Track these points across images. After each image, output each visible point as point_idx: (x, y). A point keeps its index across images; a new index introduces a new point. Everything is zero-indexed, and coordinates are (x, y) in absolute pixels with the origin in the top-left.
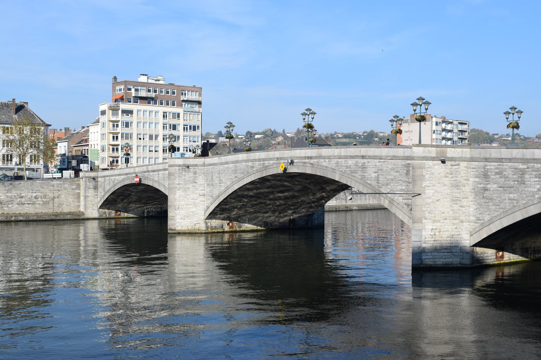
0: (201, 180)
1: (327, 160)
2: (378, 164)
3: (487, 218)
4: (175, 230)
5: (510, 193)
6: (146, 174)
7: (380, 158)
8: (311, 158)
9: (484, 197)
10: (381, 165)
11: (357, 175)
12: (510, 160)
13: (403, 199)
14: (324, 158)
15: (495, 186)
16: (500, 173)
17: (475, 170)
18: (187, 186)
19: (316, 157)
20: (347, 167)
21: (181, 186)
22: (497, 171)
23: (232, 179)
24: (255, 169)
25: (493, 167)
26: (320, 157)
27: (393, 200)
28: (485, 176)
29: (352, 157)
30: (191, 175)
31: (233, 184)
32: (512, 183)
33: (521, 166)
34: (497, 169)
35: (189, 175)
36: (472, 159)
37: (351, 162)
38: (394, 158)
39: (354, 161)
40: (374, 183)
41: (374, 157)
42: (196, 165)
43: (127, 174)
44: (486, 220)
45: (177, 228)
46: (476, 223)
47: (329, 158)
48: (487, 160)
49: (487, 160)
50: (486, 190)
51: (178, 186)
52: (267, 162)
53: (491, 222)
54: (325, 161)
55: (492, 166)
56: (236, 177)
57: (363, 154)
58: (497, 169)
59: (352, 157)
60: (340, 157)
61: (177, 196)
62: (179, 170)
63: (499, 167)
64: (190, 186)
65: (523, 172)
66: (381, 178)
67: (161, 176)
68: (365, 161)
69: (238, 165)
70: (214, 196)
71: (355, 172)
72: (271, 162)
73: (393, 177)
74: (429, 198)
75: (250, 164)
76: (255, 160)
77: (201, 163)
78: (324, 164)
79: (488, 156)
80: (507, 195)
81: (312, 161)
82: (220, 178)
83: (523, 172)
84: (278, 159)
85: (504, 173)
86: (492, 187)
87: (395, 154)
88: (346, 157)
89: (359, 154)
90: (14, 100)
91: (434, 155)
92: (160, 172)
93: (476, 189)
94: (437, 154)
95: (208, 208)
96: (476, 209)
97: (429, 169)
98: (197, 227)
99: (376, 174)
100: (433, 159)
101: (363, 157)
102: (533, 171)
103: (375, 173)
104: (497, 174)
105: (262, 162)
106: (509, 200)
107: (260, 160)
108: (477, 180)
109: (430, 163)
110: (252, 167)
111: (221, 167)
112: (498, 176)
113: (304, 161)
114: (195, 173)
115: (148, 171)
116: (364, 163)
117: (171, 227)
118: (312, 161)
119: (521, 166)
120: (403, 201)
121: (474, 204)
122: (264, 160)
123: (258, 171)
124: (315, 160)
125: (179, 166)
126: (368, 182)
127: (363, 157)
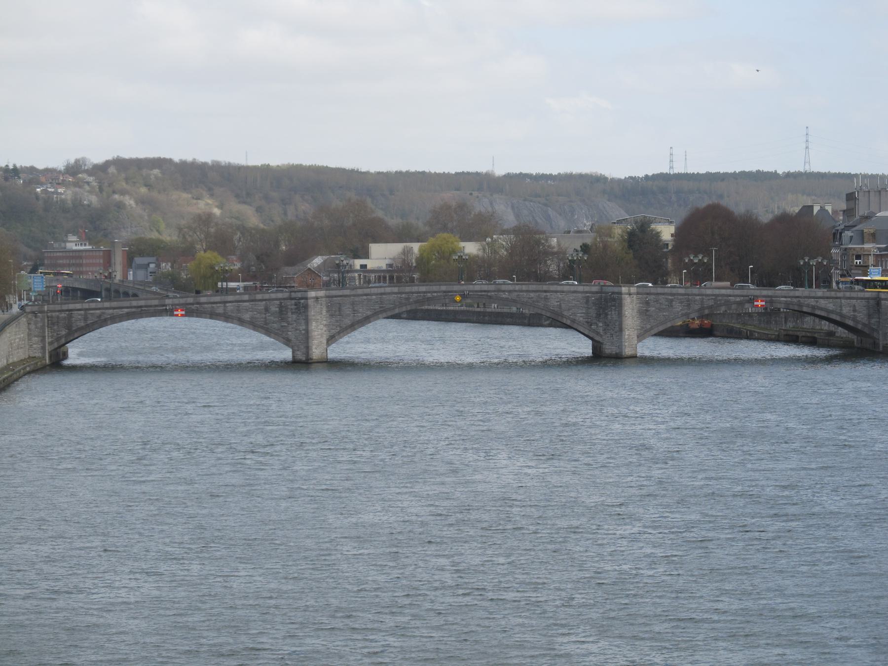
2: (560, 296)
3: (649, 326)
6: (194, 307)
7: (563, 292)
8: (488, 291)
9: (646, 315)
12: (663, 294)
14: (504, 291)
16: (657, 301)
19: (494, 291)
20: (529, 298)
24: (411, 300)
28: (647, 303)
32: (664, 307)
33: (670, 297)
37: (532, 295)
40: (556, 309)
41: (556, 292)
43: (141, 307)
47: (510, 292)
48: (648, 294)
49: (648, 294)
50: (647, 311)
55: (652, 297)
65: (672, 301)
66: (563, 306)
68: (548, 294)
69: (384, 296)
70: (344, 326)
72: (435, 294)
76: (413, 293)
78: (504, 296)
81: (489, 294)
83: (672, 301)
84: (445, 292)
92: (228, 305)
101: (545, 291)
104: (654, 302)
110: (408, 299)
111: (357, 299)
113: (480, 293)
115: (198, 303)
118: (489, 294)
119: (670, 297)
122: (425, 292)
127: (545, 291)
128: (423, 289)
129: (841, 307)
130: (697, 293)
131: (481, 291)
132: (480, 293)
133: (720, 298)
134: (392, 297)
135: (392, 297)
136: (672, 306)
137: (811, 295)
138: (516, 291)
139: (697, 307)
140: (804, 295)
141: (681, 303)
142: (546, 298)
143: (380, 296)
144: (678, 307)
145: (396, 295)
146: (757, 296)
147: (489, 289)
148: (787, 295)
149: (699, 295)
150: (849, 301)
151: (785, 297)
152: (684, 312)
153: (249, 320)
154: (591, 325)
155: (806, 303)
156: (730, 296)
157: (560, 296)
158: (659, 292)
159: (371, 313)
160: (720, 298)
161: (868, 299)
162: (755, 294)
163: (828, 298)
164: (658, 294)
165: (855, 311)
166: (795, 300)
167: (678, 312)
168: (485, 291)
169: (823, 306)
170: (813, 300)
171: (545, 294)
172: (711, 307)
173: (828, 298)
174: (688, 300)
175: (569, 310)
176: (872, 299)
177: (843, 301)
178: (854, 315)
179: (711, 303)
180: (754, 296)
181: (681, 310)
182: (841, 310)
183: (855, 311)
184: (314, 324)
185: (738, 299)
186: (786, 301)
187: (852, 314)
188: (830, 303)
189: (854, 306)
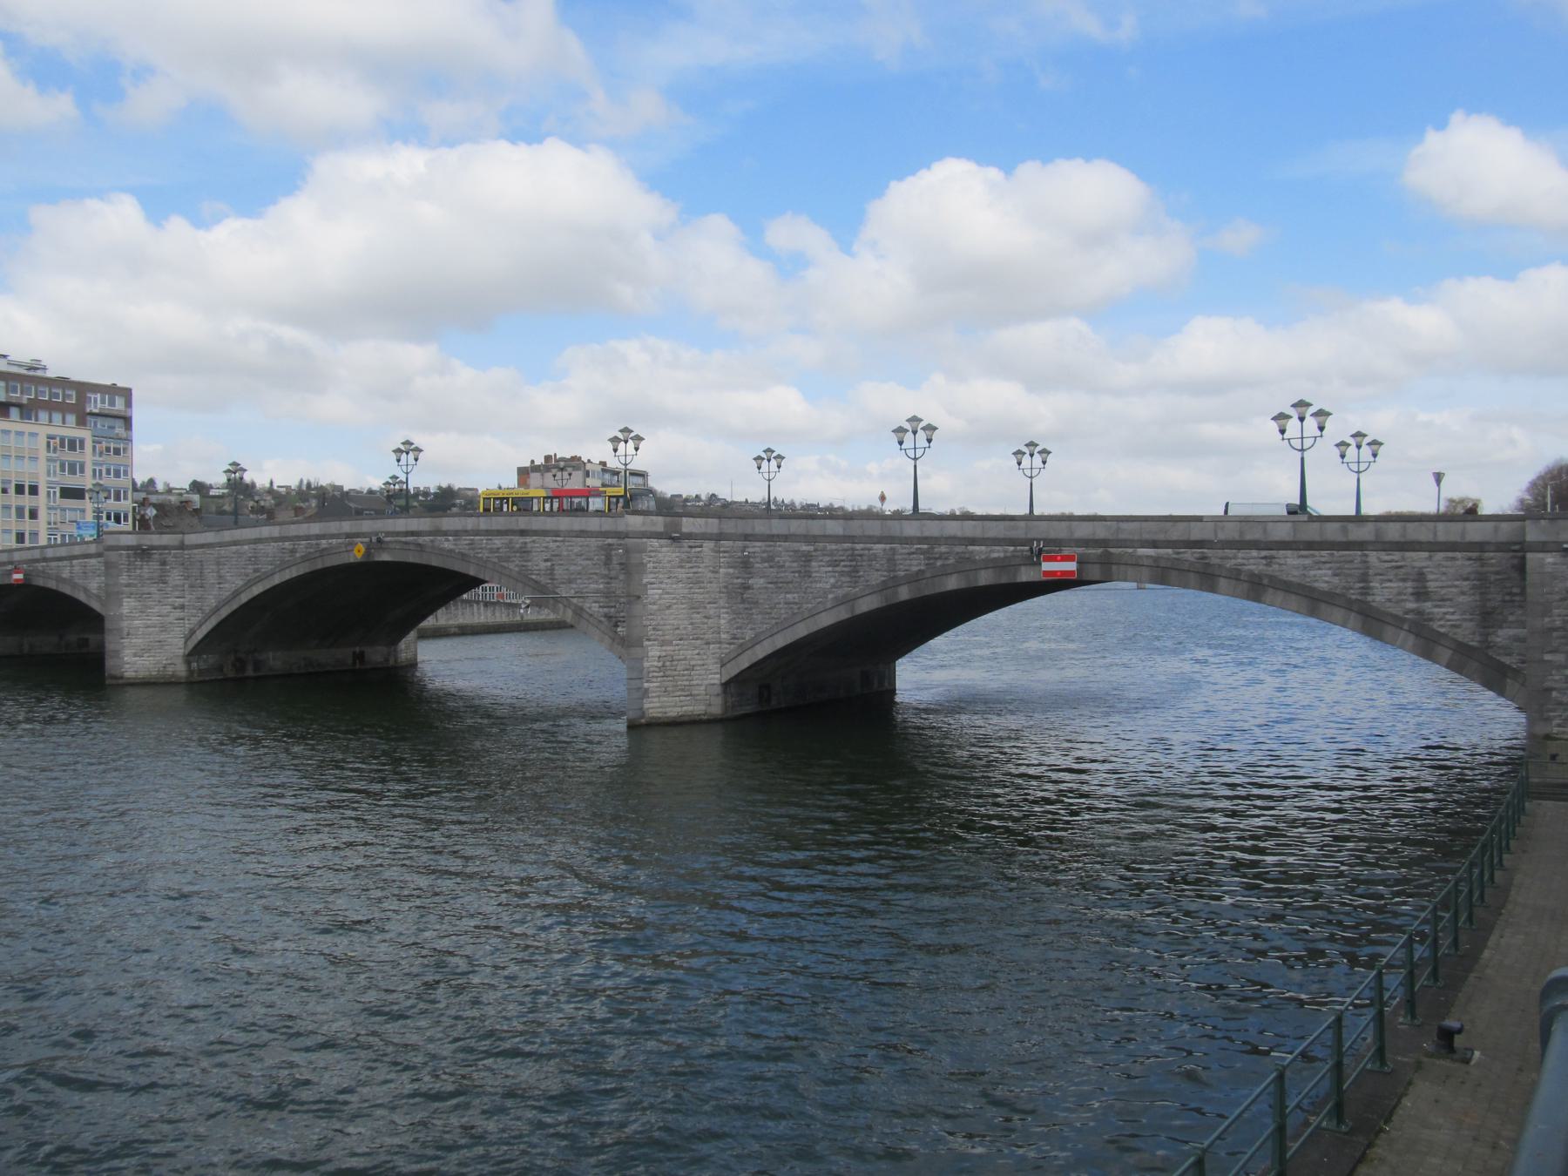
0: (175, 577)
1: (450, 538)
2: (552, 545)
3: (749, 634)
4: (122, 678)
5: (786, 593)
6: (40, 566)
7: (556, 533)
9: (743, 601)
10: (558, 547)
11: (511, 566)
12: (786, 538)
13: (600, 607)
14: (445, 533)
15: (762, 581)
16: (770, 559)
17: (726, 555)
18: (146, 590)
19: (430, 533)
20: (491, 551)
21: (133, 589)
22: (765, 555)
23: (247, 576)
24: (298, 555)
25: (757, 549)
26: (437, 532)
27: (582, 609)
28: (745, 565)
29: (500, 533)
30: (155, 565)
31: (249, 584)
32: (790, 576)
33: (804, 548)
34: (764, 552)
35: (149, 569)
36: (719, 537)
37: (498, 542)
38: (582, 534)
39: (506, 539)
40: (544, 580)
41: (545, 533)
42: (165, 547)
44: (747, 638)
45: (127, 675)
46: (730, 644)
47: (457, 534)
49: (747, 537)
50: (747, 588)
51: (126, 589)
52: (324, 541)
53: (756, 641)
54: (448, 540)
55: (756, 547)
56: (256, 571)
57: (522, 526)
58: (764, 552)
59: (500, 533)
60: (477, 533)
61: (125, 610)
62: (128, 556)
63: (768, 549)
64: (153, 589)
65: (807, 558)
66: (559, 571)
67: (77, 569)
68: (528, 539)
69: (260, 546)
70: (207, 609)
71: (508, 559)
73: (580, 568)
74: (654, 604)
75: (287, 544)
76: (299, 538)
77: (176, 543)
78: (446, 545)
79: (749, 531)
80: (782, 596)
81: (421, 540)
82: (218, 572)
83: (807, 558)
84: (348, 536)
85: (777, 559)
86: (756, 582)
87: (583, 528)
88: (488, 533)
89: (516, 528)
90: (533, 462)
91: (660, 528)
92: (75, 562)
93: (730, 587)
94: (665, 526)
95: (193, 632)
96: (731, 620)
97: (653, 554)
98: (170, 670)
99: (549, 564)
100: (658, 536)
101: (523, 533)
102: (824, 555)
103: (546, 560)
104: (764, 560)
105: (314, 542)
106: (786, 603)
107: (308, 538)
108: (731, 571)
109: (655, 543)
110: (293, 551)
111: (223, 551)
112: (766, 564)
113: (403, 539)
114: (164, 563)
115: (45, 560)
116: (526, 543)
117: (113, 672)
118: (421, 540)
119: (804, 548)
120: (601, 610)
121: (727, 613)
122: (319, 537)
123: (305, 559)
124: (427, 538)
125: (128, 548)
126: (534, 577)
127: (523, 533)
128: (315, 528)
129: (1364, 578)
130: (877, 533)
131: (408, 534)
132: (403, 539)
133: (943, 549)
134: (271, 548)
135: (271, 548)
136: (808, 574)
137: (1248, 537)
138: (466, 532)
139: (876, 578)
140: (1221, 536)
141: (834, 564)
142: (524, 552)
143: (252, 546)
144: (825, 579)
145: (275, 544)
146: (1058, 543)
147: (421, 528)
148: (1161, 537)
149: (880, 540)
150: (1397, 555)
151: (1154, 544)
152: (840, 592)
153: (95, 592)
154: (616, 626)
155: (1229, 564)
156: (973, 541)
157: (552, 545)
158: (775, 532)
159: (241, 583)
160: (943, 549)
161: (1480, 546)
162: (1053, 535)
163: (1310, 545)
164: (771, 538)
165: (1421, 594)
166: (1189, 555)
167: (826, 593)
168: (412, 533)
169: (1294, 576)
170: (1254, 553)
171: (522, 540)
172: (914, 579)
173: (1310, 545)
174: (853, 557)
175: (570, 581)
176: (1501, 547)
177: (1373, 557)
178: (1419, 612)
179: (917, 564)
180: (1048, 542)
181: (833, 586)
182: (1366, 591)
183: (1421, 594)
184: (128, 605)
185: (998, 553)
186: (1156, 559)
187: (1411, 605)
188: (1319, 564)
189: (1421, 577)
